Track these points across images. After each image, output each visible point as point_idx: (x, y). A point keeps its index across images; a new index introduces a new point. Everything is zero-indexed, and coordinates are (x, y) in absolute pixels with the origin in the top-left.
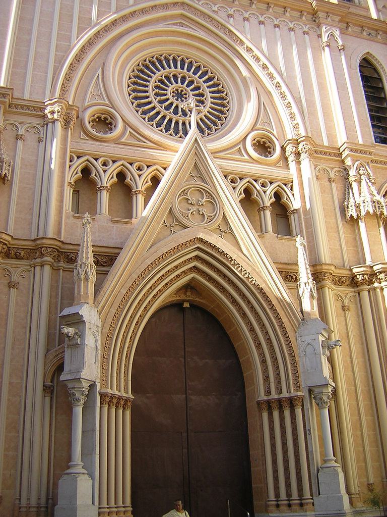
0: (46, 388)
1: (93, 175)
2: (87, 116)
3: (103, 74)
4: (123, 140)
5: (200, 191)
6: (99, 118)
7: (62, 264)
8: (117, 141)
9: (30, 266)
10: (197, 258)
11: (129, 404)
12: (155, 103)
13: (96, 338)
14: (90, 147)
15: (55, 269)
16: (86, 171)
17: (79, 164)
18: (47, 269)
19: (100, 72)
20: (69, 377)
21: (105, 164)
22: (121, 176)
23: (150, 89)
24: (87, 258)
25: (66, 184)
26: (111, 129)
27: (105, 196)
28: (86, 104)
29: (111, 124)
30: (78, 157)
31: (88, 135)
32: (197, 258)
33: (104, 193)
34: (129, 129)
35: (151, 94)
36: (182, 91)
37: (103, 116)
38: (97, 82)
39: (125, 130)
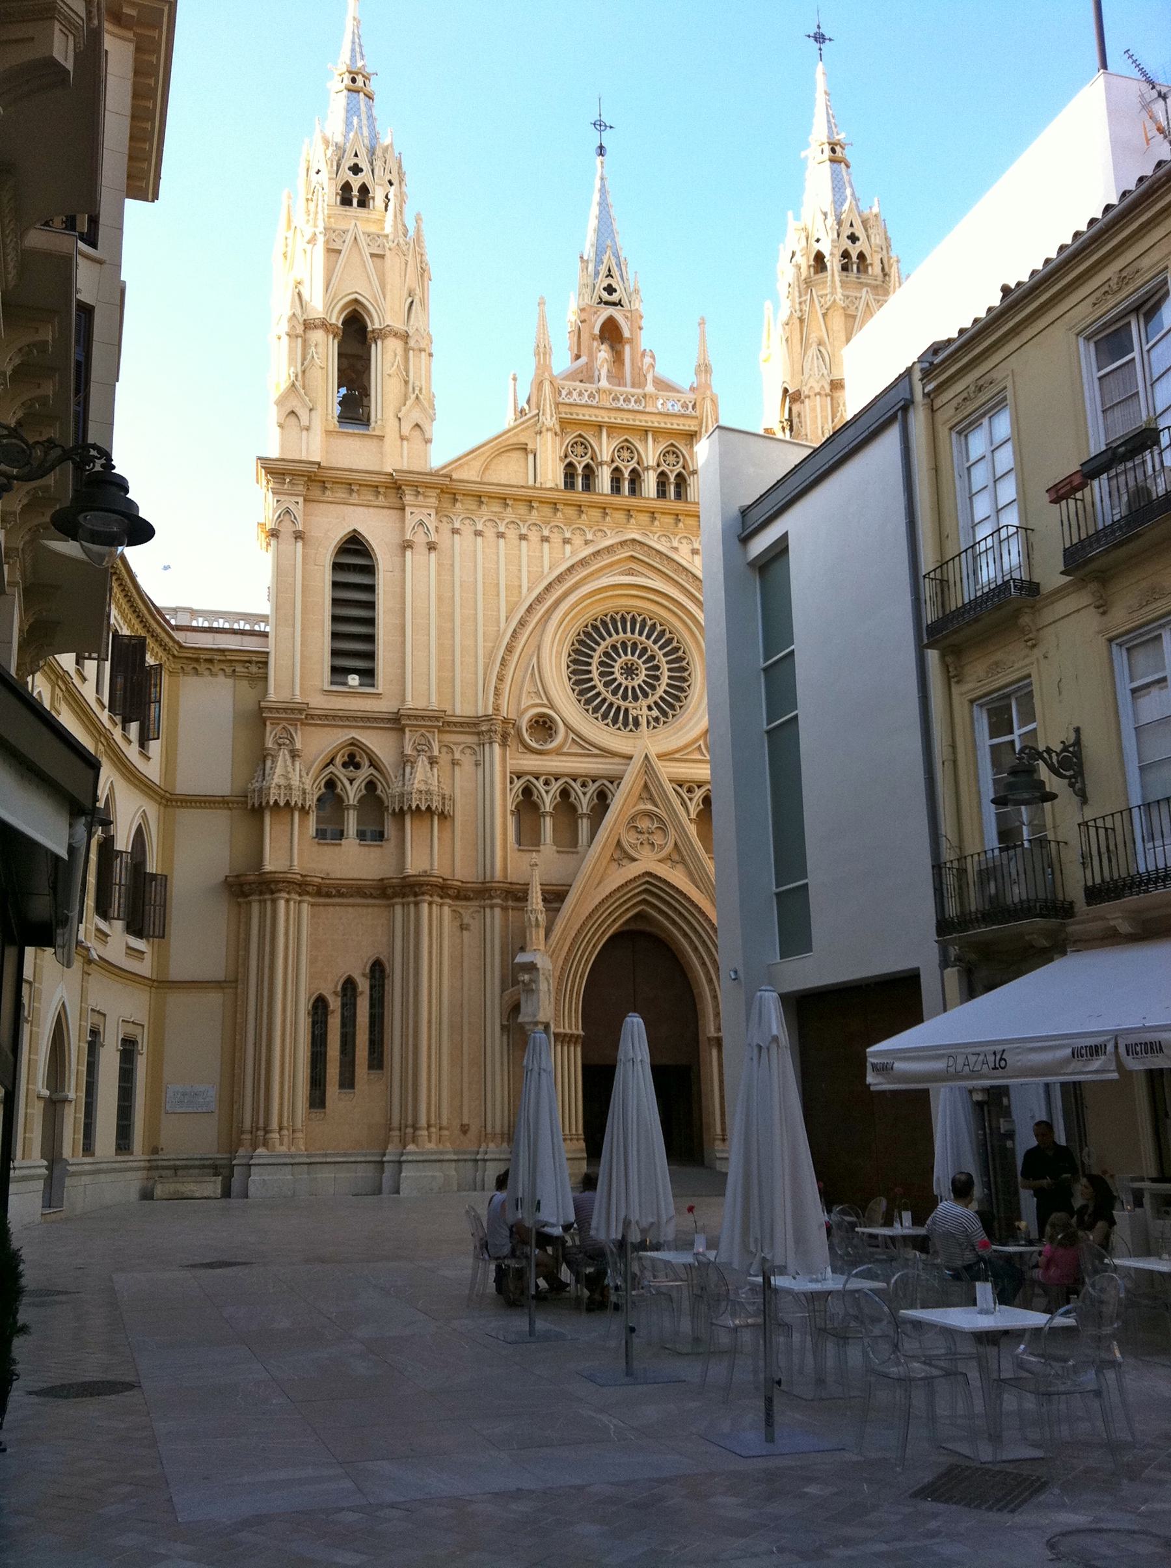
0: (503, 1027)
1: (535, 798)
2: (524, 724)
3: (538, 662)
4: (565, 750)
5: (649, 815)
6: (537, 722)
7: (510, 903)
8: (558, 752)
9: (480, 906)
10: (646, 891)
11: (580, 1041)
12: (600, 687)
13: (548, 982)
14: (531, 763)
15: (504, 909)
16: (527, 791)
17: (519, 784)
18: (497, 911)
19: (535, 660)
20: (527, 1019)
21: (546, 783)
22: (565, 793)
23: (594, 668)
24: (536, 900)
25: (509, 812)
26: (551, 736)
27: (548, 822)
28: (523, 707)
29: (550, 728)
30: (518, 778)
31: (526, 748)
32: (646, 891)
33: (548, 820)
34: (572, 735)
35: (595, 674)
36: (632, 664)
37: (541, 720)
38: (533, 674)
39: (567, 736)
